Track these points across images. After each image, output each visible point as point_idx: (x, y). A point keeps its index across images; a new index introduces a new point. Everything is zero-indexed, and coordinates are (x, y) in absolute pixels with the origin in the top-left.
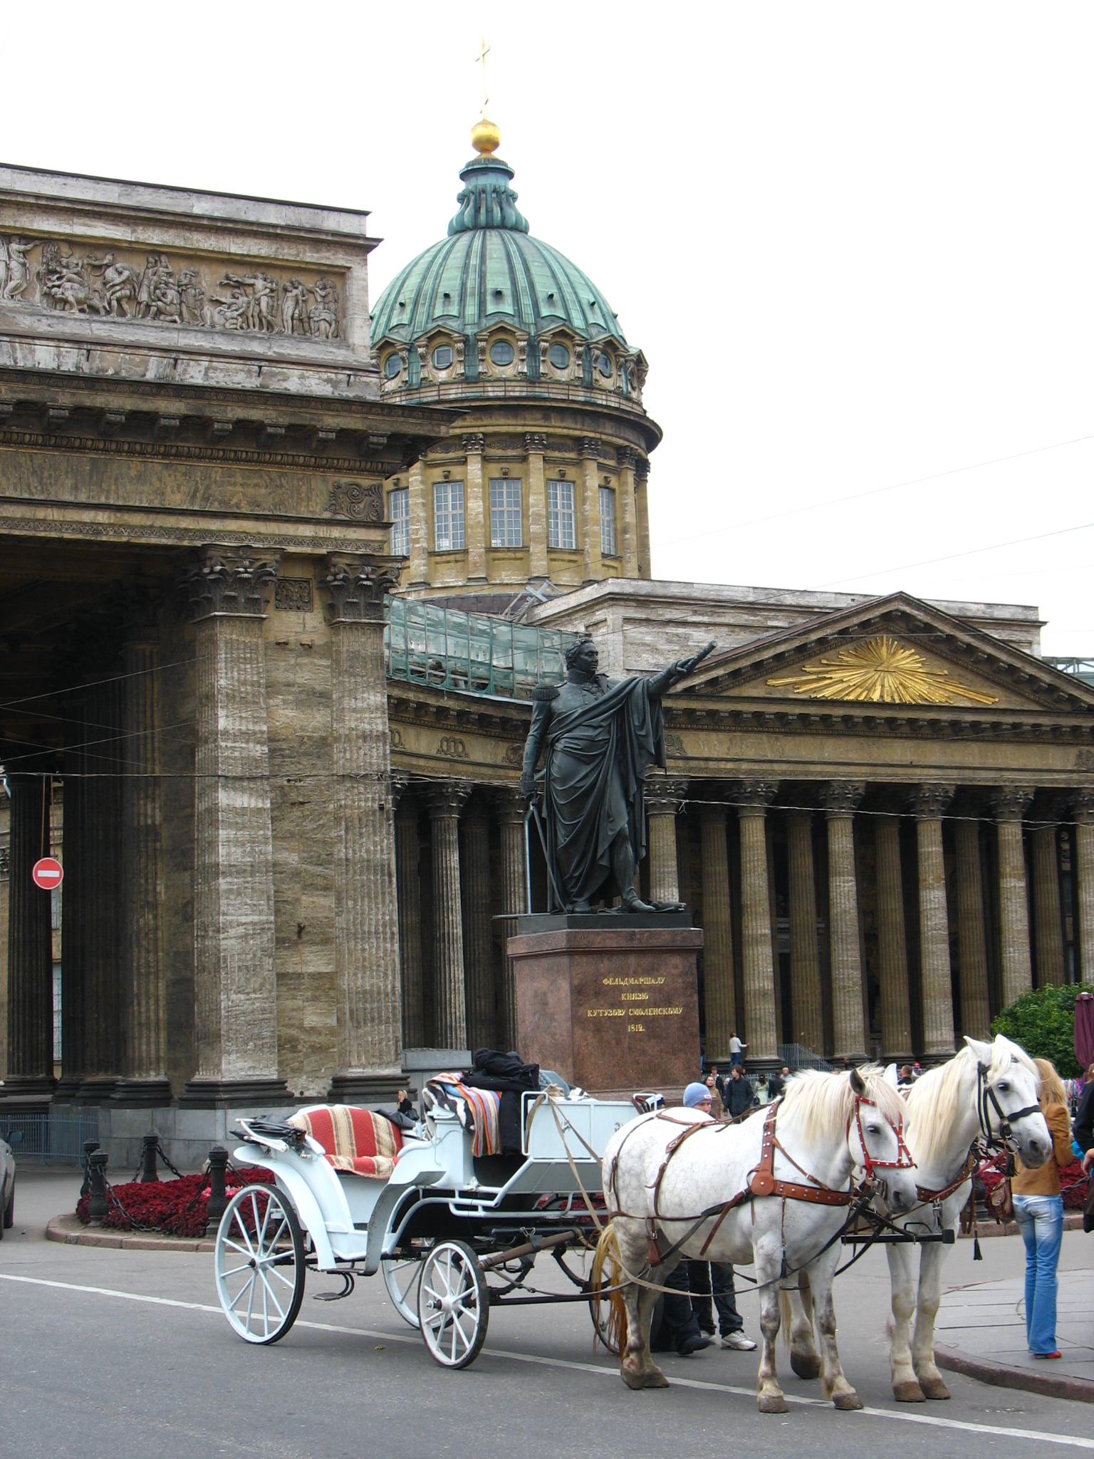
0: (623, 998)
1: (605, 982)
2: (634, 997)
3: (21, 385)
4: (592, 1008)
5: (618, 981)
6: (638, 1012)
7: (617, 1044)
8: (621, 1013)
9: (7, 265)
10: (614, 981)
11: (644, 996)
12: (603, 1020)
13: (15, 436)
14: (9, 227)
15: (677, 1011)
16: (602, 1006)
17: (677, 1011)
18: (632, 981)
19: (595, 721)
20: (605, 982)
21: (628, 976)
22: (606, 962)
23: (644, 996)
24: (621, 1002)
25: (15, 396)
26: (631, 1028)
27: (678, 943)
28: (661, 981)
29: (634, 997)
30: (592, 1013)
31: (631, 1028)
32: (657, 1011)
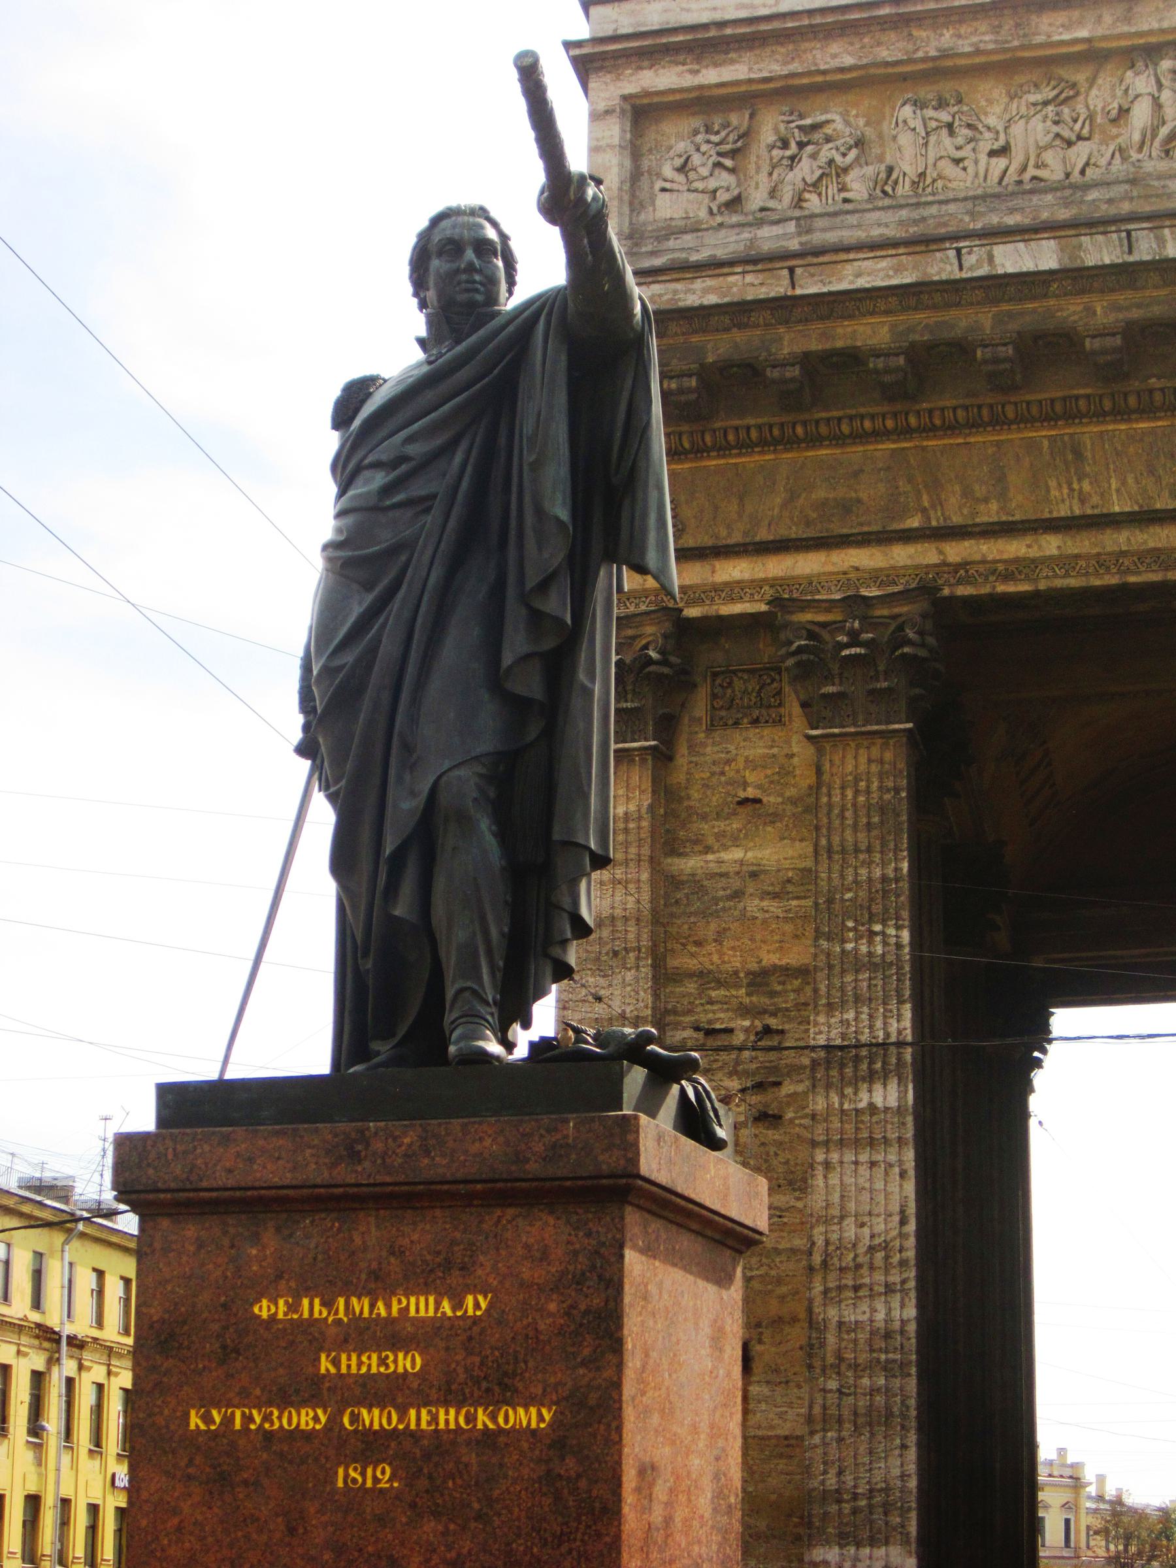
0: (325, 1365)
1: (263, 1309)
2: (371, 1363)
3: (1129, 294)
4: (207, 1403)
5: (312, 1308)
6: (373, 1418)
7: (292, 1531)
8: (306, 1419)
9: (1157, 105)
10: (294, 1307)
11: (407, 1362)
12: (242, 1442)
13: (1158, 397)
14: (1151, 32)
15: (524, 1417)
16: (245, 1398)
17: (524, 1417)
18: (361, 1306)
19: (384, 452)
20: (263, 1309)
21: (349, 1290)
22: (271, 1241)
23: (407, 1362)
24: (318, 1380)
25: (1121, 316)
26: (347, 1475)
27: (533, 1167)
28: (474, 1305)
29: (371, 1363)
30: (207, 1419)
31: (347, 1475)
32: (449, 1418)
